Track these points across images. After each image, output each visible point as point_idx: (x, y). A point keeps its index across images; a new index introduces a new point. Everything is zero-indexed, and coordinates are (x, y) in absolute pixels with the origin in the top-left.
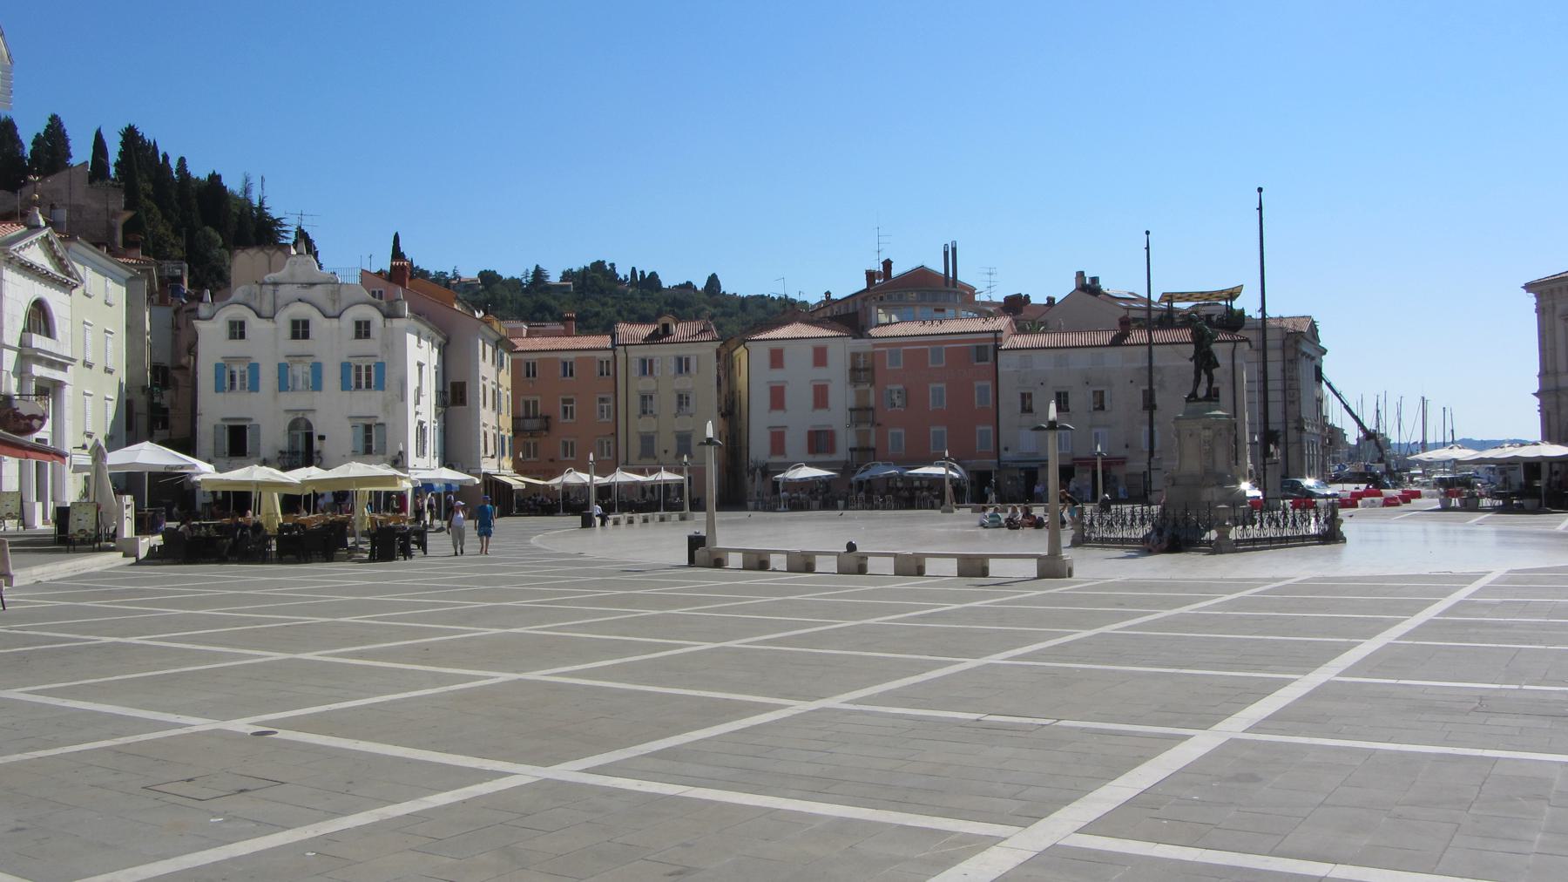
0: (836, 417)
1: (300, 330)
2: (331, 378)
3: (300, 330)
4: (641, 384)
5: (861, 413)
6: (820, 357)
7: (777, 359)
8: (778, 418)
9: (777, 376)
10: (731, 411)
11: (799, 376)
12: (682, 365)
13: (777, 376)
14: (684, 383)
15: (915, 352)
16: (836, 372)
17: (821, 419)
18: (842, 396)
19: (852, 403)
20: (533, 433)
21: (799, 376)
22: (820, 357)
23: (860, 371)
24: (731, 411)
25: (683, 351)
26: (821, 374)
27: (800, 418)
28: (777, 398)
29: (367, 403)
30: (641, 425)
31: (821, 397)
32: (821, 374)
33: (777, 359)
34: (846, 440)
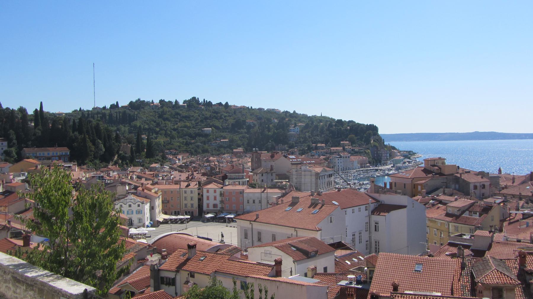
0: (218, 202)
1: (130, 206)
2: (135, 212)
3: (130, 206)
4: (184, 195)
5: (222, 202)
6: (215, 191)
7: (208, 191)
8: (208, 202)
9: (208, 194)
10: (200, 200)
11: (211, 194)
12: (191, 192)
13: (208, 194)
14: (192, 195)
15: (231, 192)
16: (218, 194)
17: (215, 202)
18: (219, 198)
19: (220, 200)
20: (166, 203)
21: (211, 194)
22: (215, 191)
23: (221, 194)
24: (200, 200)
25: (192, 189)
26: (215, 194)
27: (212, 202)
28: (208, 198)
29: (140, 216)
30: (185, 202)
31: (215, 198)
32: (215, 194)
33: (208, 191)
34: (219, 206)
